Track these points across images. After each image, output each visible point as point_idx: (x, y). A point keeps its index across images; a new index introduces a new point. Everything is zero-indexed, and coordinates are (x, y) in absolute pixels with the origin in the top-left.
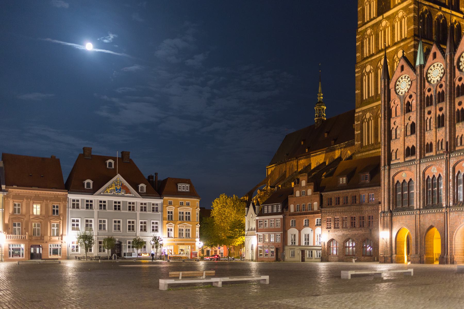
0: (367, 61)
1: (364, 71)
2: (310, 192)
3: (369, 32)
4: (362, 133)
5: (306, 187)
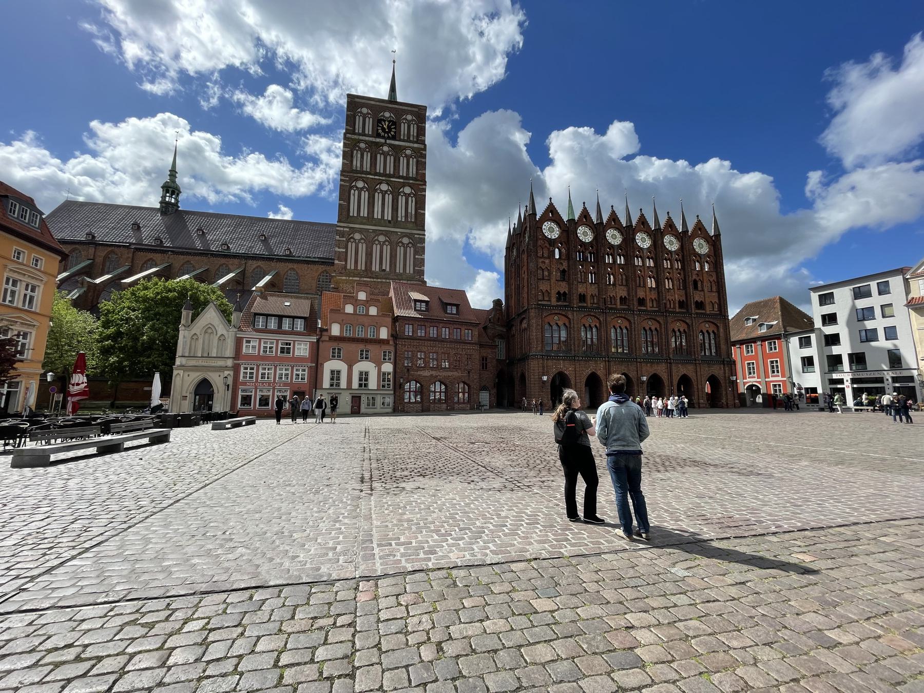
0: (359, 175)
1: (354, 184)
2: (373, 311)
3: (362, 145)
4: (346, 252)
5: (367, 303)
